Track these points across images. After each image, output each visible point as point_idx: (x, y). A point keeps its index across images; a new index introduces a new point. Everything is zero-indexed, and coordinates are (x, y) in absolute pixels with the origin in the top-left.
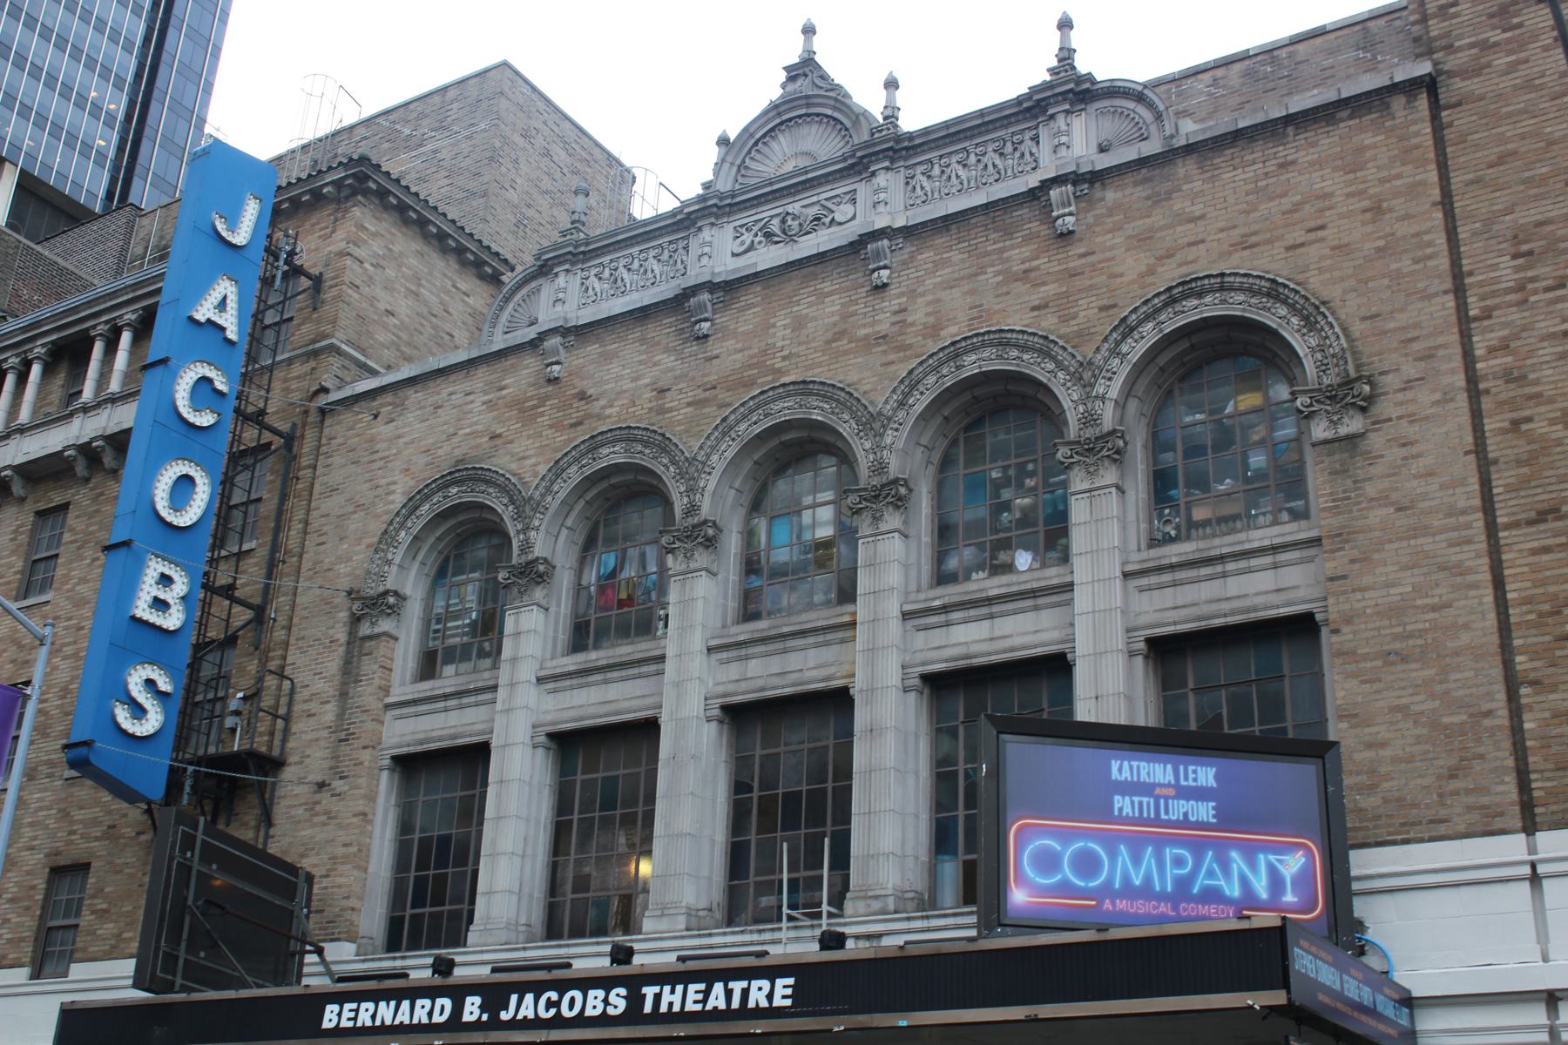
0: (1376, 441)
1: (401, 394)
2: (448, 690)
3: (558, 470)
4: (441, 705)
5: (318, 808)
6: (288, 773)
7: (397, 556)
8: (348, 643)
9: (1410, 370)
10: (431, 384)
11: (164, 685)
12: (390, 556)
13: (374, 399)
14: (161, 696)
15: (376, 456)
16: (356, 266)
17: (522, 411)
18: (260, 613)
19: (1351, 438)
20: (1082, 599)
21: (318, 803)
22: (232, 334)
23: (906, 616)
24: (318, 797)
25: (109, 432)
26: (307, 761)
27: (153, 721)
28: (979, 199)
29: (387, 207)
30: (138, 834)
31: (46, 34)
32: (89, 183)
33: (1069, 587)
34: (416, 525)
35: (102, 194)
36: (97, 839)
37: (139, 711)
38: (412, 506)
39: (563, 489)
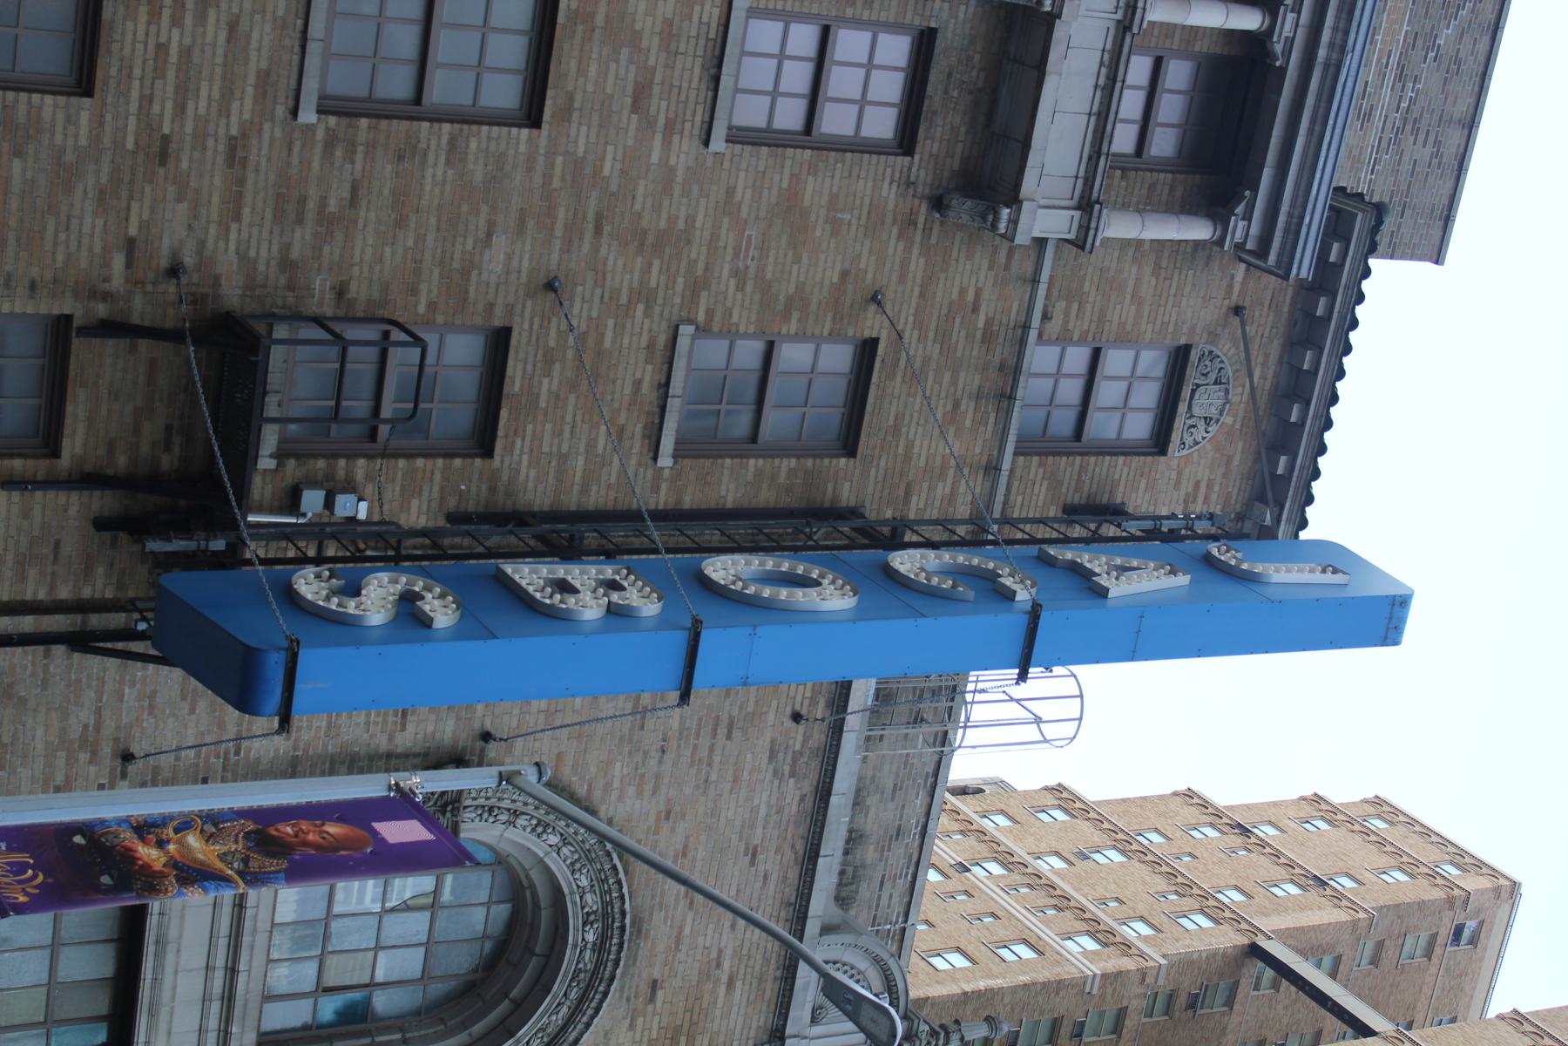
1: (815, 764)
2: (242, 980)
4: (220, 960)
5: (84, 757)
8: (389, 756)
10: (802, 830)
12: (521, 821)
13: (830, 704)
15: (722, 732)
17: (677, 1031)
21: (94, 753)
24: (106, 749)
25: (1060, 31)
26: (186, 706)
30: (130, 245)
36: (147, 100)
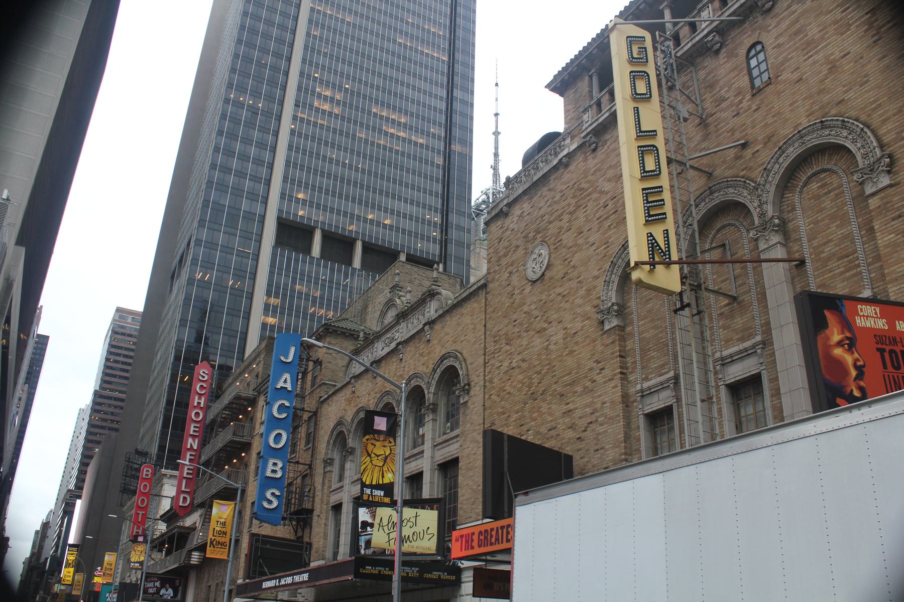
0: (469, 403)
3: (353, 420)
6: (315, 513)
7: (330, 447)
9: (476, 381)
11: (278, 493)
14: (277, 497)
16: (330, 356)
18: (310, 466)
19: (467, 402)
20: (425, 454)
22: (290, 389)
23: (405, 459)
27: (275, 503)
28: (415, 331)
29: (339, 335)
31: (406, 201)
32: (434, 249)
33: (422, 452)
34: (334, 437)
35: (437, 252)
37: (270, 502)
38: (332, 432)
39: (354, 425)
